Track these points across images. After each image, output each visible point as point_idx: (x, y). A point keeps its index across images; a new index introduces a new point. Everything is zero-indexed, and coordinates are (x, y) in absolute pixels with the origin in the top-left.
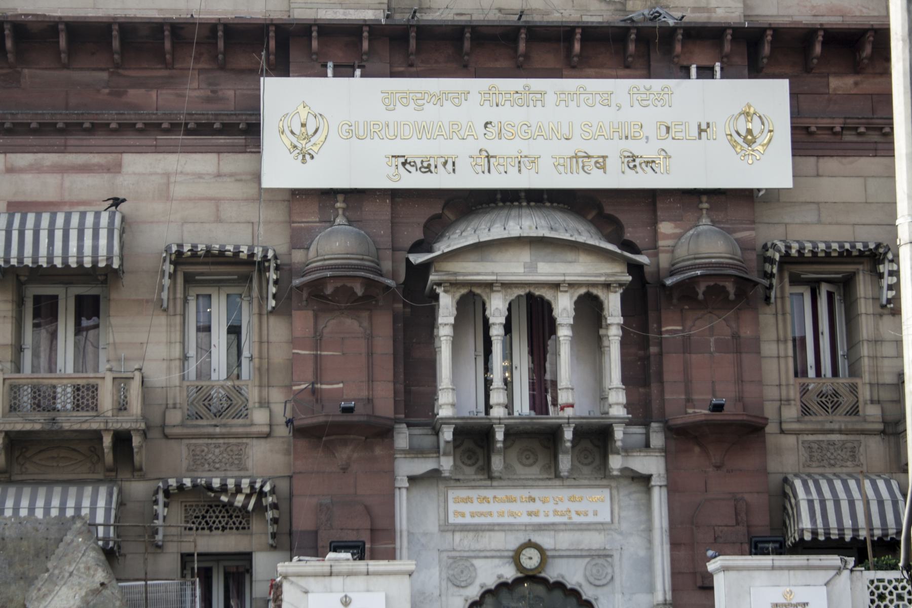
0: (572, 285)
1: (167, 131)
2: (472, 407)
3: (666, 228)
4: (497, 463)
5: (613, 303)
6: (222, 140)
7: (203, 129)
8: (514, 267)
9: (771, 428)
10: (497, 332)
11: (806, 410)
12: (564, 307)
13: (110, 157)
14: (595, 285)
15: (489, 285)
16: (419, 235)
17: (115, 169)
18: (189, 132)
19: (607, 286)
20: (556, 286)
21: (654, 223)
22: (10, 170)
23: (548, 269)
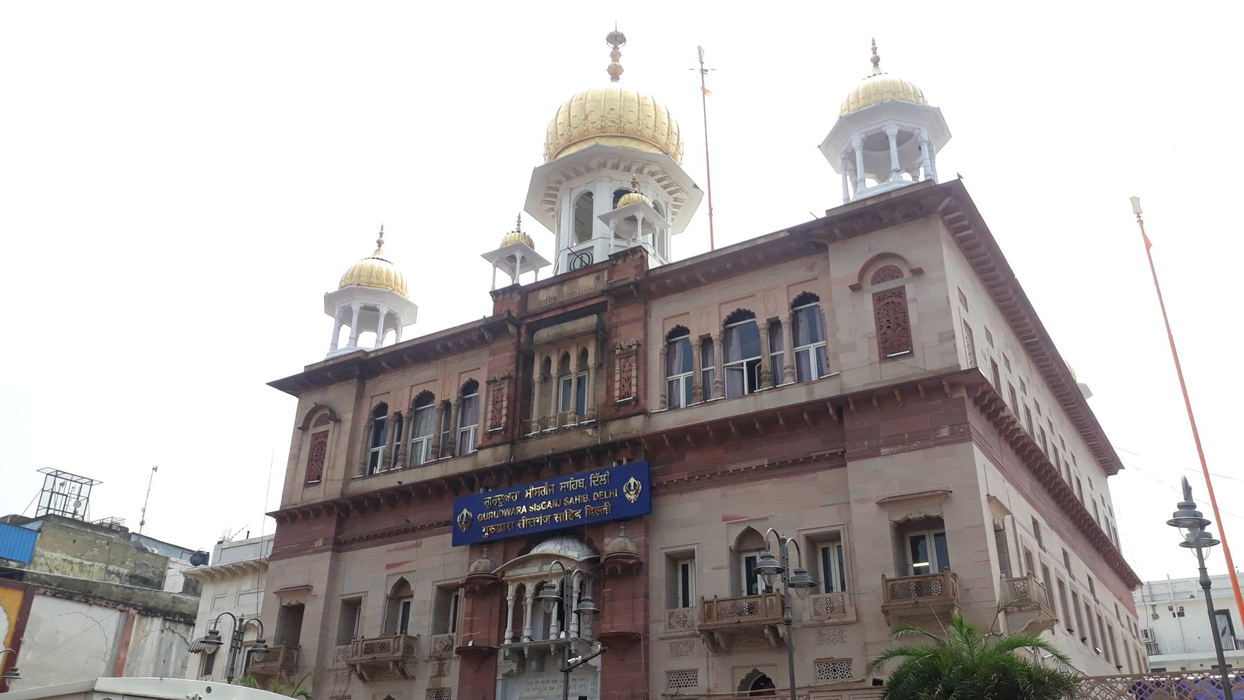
2: (539, 639)
9: (653, 638)
11: (671, 626)
15: (524, 579)
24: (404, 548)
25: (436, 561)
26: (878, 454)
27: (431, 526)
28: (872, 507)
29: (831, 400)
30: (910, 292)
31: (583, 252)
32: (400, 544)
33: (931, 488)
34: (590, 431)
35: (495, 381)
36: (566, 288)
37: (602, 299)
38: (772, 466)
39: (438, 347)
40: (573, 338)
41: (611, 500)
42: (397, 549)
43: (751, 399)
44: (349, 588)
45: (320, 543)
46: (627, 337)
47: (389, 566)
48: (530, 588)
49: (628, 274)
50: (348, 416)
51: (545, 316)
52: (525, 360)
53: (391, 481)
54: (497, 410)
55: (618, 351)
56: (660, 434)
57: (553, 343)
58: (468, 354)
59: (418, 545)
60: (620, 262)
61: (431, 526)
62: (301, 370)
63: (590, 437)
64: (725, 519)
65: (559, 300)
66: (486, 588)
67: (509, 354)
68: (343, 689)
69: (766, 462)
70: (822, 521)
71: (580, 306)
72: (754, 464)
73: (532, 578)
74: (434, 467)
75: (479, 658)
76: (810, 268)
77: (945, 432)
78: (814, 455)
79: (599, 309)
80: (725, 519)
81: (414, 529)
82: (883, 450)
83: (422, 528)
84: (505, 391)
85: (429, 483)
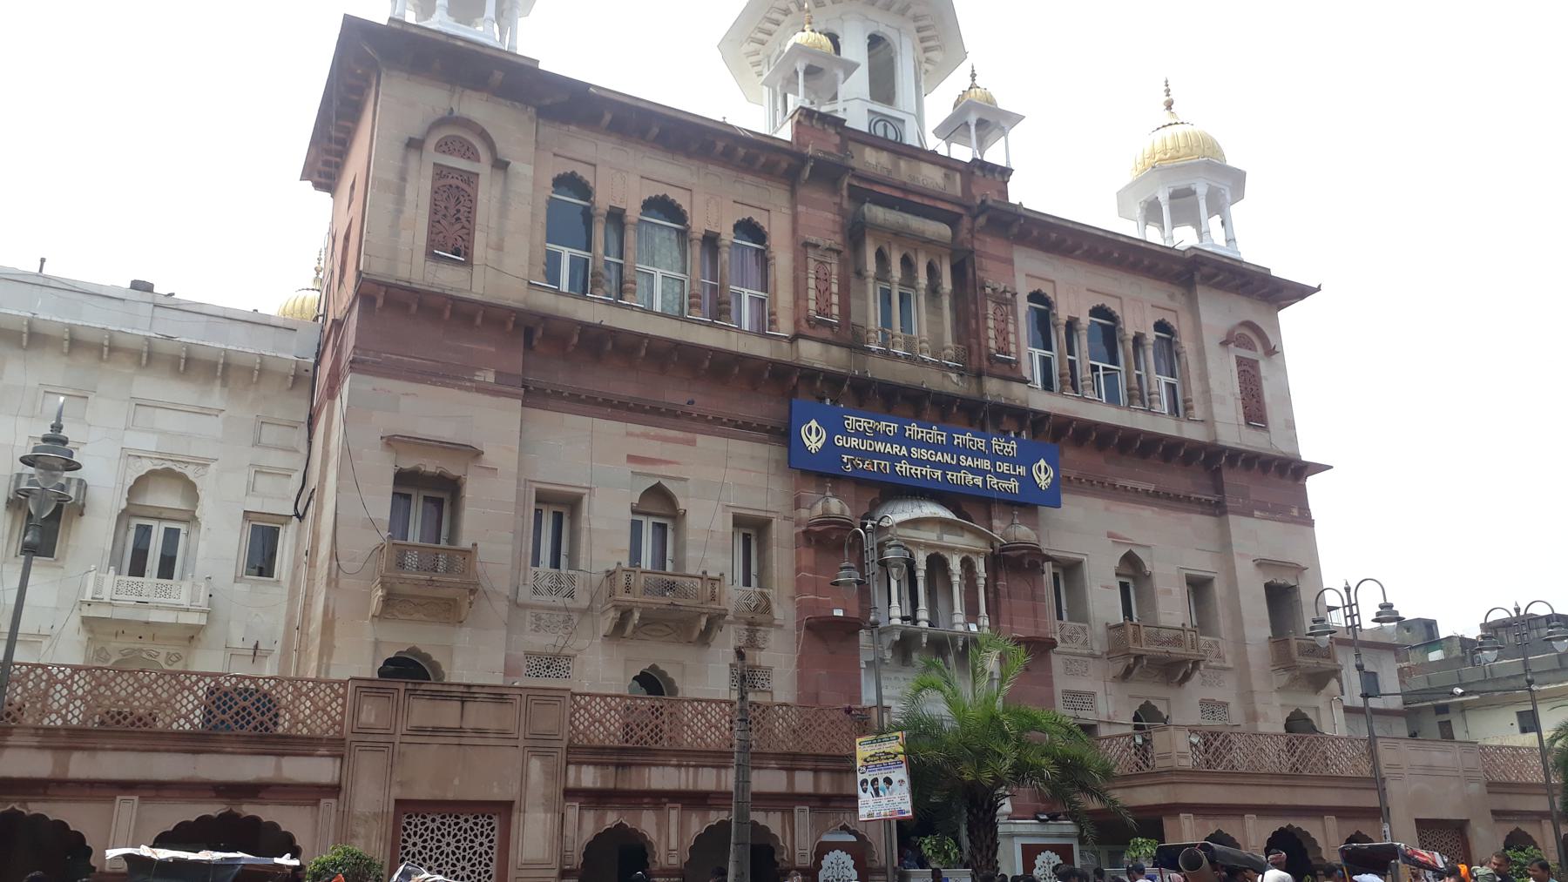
0: (962, 550)
1: (724, 424)
3: (996, 523)
4: (915, 656)
5: (980, 566)
6: (754, 434)
7: (746, 426)
8: (929, 536)
10: (921, 574)
12: (955, 564)
13: (689, 435)
14: (971, 552)
15: (918, 544)
16: (867, 509)
17: (692, 443)
18: (737, 426)
19: (978, 553)
20: (952, 550)
21: (990, 519)
22: (629, 434)
23: (950, 539)
24: (665, 439)
25: (723, 478)
26: (1252, 516)
27: (717, 420)
28: (1251, 565)
29: (1231, 449)
30: (1263, 365)
31: (886, 119)
32: (652, 430)
33: (1290, 560)
34: (954, 377)
35: (816, 246)
36: (903, 164)
37: (957, 210)
38: (1156, 494)
39: (720, 145)
40: (927, 242)
41: (1018, 477)
42: (646, 436)
43: (1126, 412)
44: (560, 473)
45: (491, 378)
46: (991, 275)
47: (632, 459)
48: (921, 558)
49: (982, 191)
50: (522, 169)
51: (876, 188)
52: (855, 232)
53: (591, 312)
54: (824, 293)
55: (988, 290)
56: (872, 381)
57: (899, 234)
58: (748, 178)
59: (692, 443)
60: (978, 173)
61: (717, 420)
62: (384, 22)
63: (953, 384)
64: (1110, 535)
65: (894, 176)
66: (826, 540)
67: (830, 216)
68: (561, 643)
69: (1152, 488)
70: (1202, 564)
71: (926, 202)
72: (1141, 486)
73: (927, 546)
74: (703, 329)
75: (830, 635)
76: (1172, 297)
77: (1295, 512)
78: (1193, 496)
79: (952, 220)
80: (1110, 535)
81: (688, 415)
82: (1257, 513)
83: (702, 418)
84: (835, 269)
85: (613, 333)
